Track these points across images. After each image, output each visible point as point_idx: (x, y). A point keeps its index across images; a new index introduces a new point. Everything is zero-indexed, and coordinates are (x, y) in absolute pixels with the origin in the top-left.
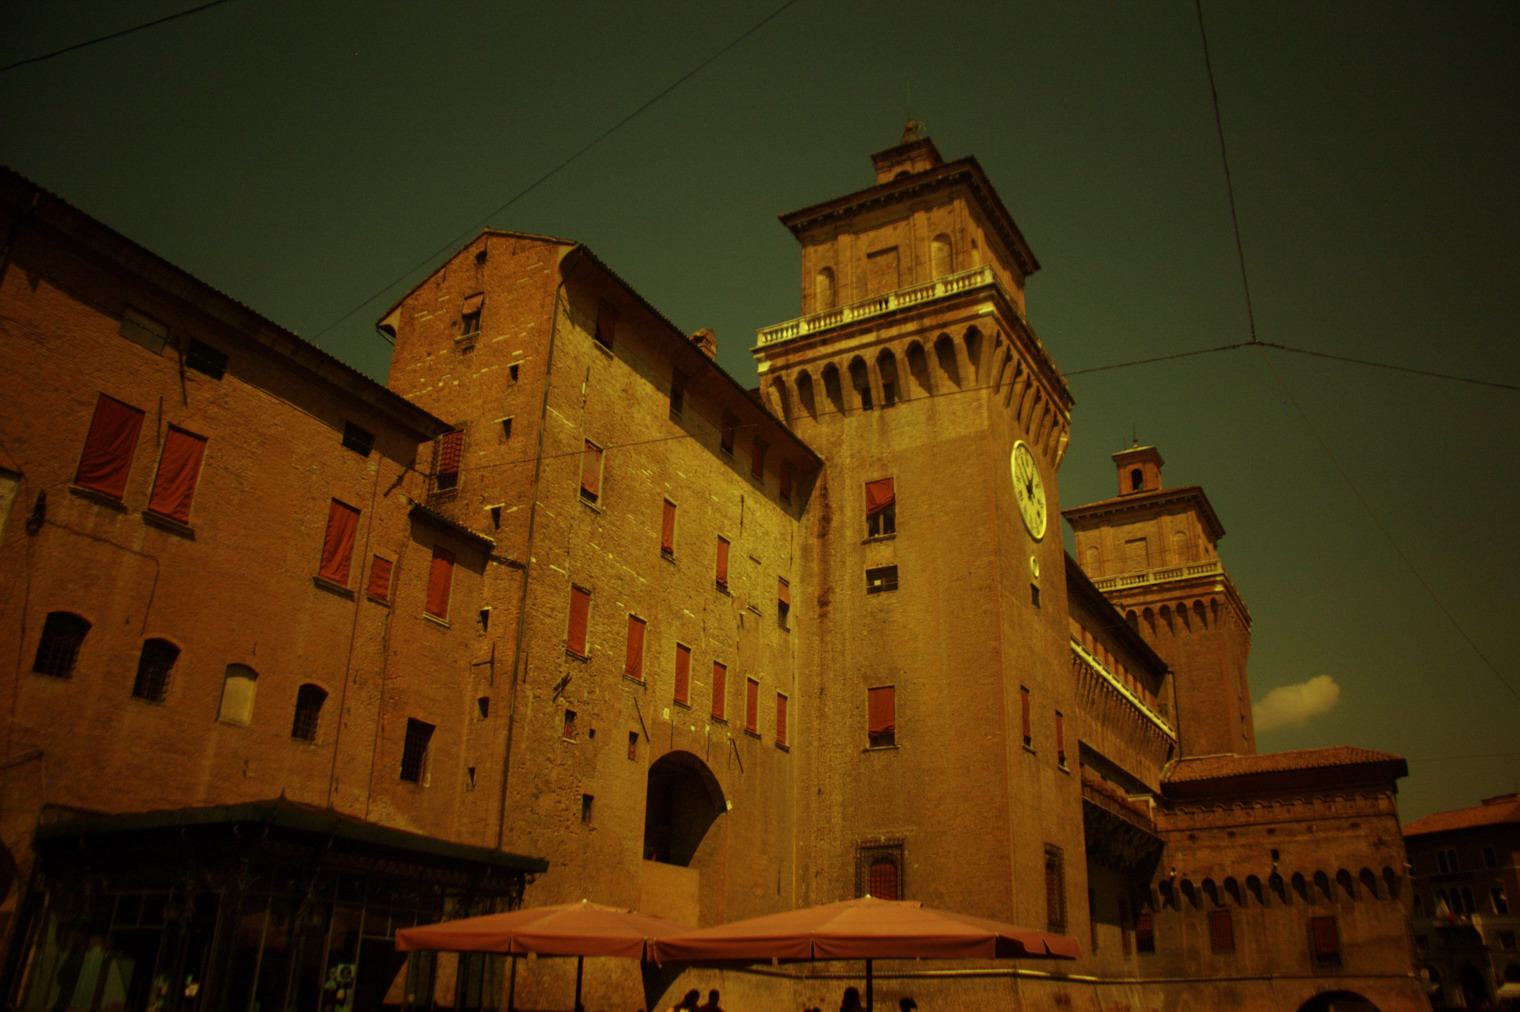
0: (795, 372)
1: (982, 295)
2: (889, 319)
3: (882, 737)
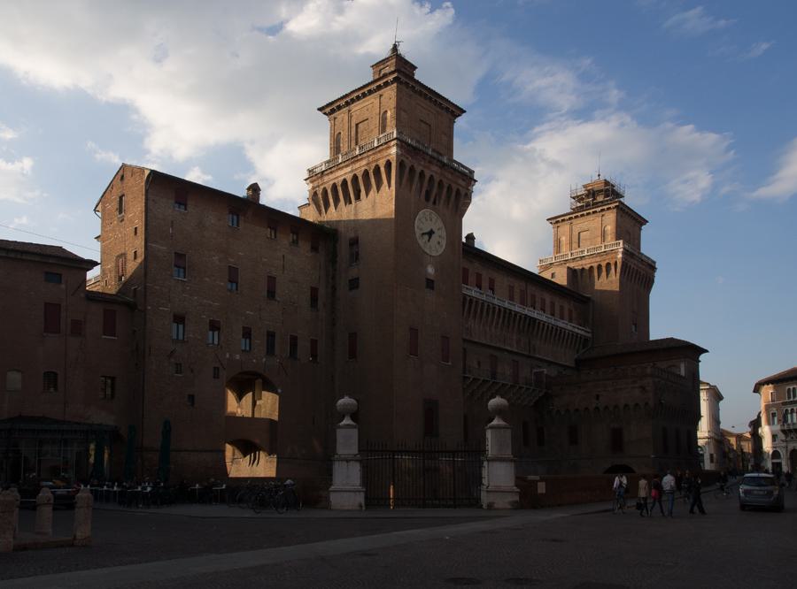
0: (322, 187)
1: (393, 143)
3: (353, 354)
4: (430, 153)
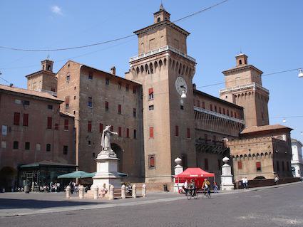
2: (151, 56)
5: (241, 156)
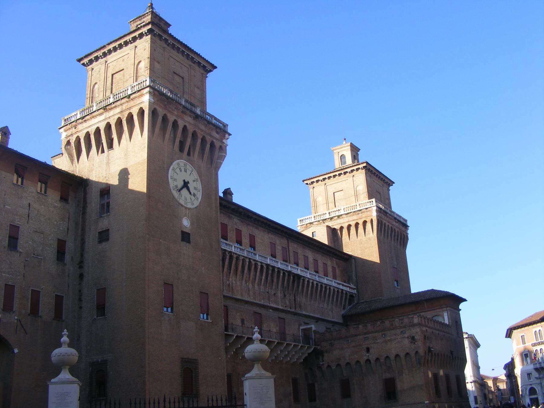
4: (183, 103)
5: (348, 364)
